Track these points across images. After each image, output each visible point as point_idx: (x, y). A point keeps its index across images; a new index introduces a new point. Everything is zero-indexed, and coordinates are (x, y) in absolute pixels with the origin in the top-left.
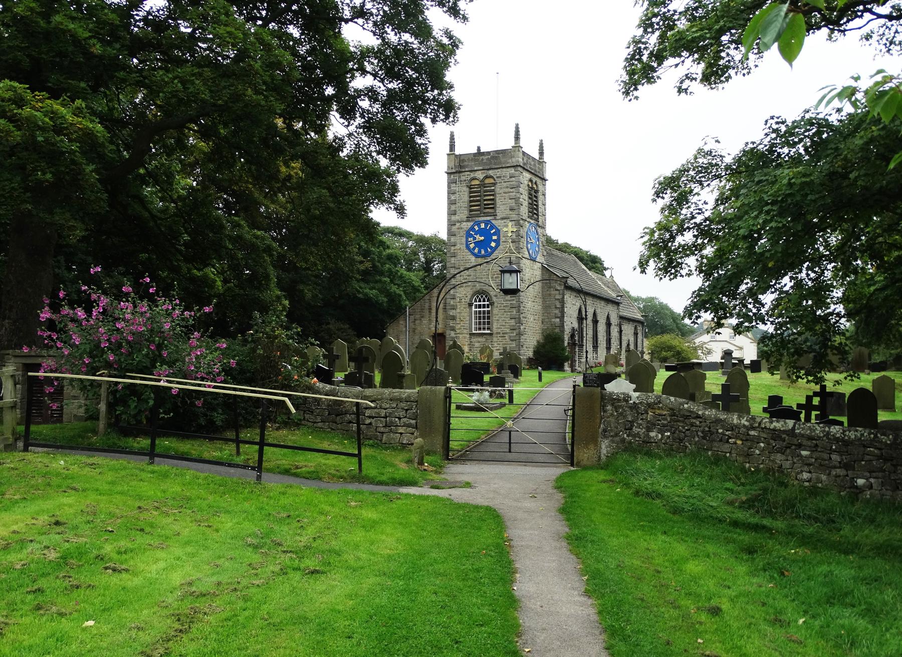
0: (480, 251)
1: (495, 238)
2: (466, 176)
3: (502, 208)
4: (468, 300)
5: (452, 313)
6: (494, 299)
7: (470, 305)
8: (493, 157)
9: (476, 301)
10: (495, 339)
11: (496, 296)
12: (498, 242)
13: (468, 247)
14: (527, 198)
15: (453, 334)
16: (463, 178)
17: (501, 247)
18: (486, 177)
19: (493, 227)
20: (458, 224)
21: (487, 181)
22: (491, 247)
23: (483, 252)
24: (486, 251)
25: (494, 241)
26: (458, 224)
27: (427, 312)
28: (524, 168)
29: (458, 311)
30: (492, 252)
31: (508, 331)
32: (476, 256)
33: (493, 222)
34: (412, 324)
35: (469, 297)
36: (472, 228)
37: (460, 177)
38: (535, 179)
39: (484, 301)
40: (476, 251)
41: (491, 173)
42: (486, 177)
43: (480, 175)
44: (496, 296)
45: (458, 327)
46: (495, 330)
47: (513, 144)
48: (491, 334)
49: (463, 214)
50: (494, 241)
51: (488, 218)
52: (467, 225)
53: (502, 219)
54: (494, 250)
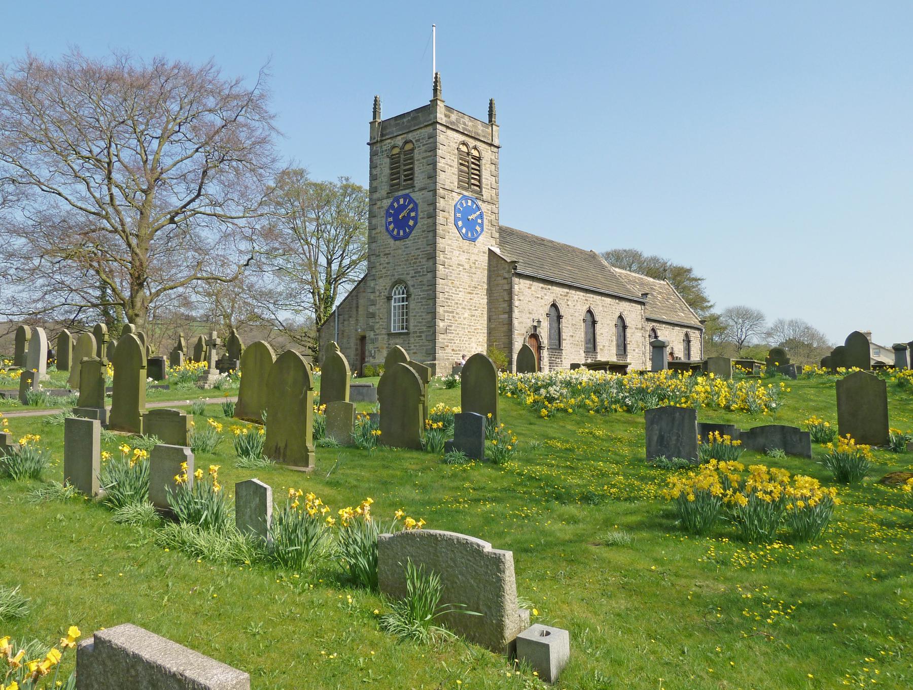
0: (398, 233)
1: (413, 214)
2: (388, 143)
3: (420, 179)
4: (386, 294)
5: (372, 309)
6: (411, 289)
7: (389, 298)
8: (414, 118)
9: (395, 294)
10: (412, 340)
11: (413, 286)
12: (415, 219)
13: (387, 229)
14: (455, 164)
15: (372, 333)
16: (384, 148)
17: (419, 224)
18: (406, 143)
19: (412, 201)
20: (379, 203)
21: (409, 147)
22: (409, 227)
23: (401, 233)
24: (405, 231)
25: (413, 218)
26: (379, 203)
27: (354, 310)
28: (447, 127)
29: (378, 307)
30: (410, 232)
31: (424, 329)
32: (396, 238)
33: (412, 195)
34: (340, 326)
35: (388, 288)
36: (392, 206)
37: (381, 147)
38: (472, 143)
39: (403, 293)
40: (395, 232)
41: (410, 136)
42: (406, 143)
43: (399, 141)
44: (413, 286)
45: (377, 326)
46: (412, 328)
47: (432, 98)
48: (407, 334)
49: (383, 190)
50: (413, 218)
51: (407, 191)
52: (386, 203)
53: (421, 190)
54: (412, 228)
